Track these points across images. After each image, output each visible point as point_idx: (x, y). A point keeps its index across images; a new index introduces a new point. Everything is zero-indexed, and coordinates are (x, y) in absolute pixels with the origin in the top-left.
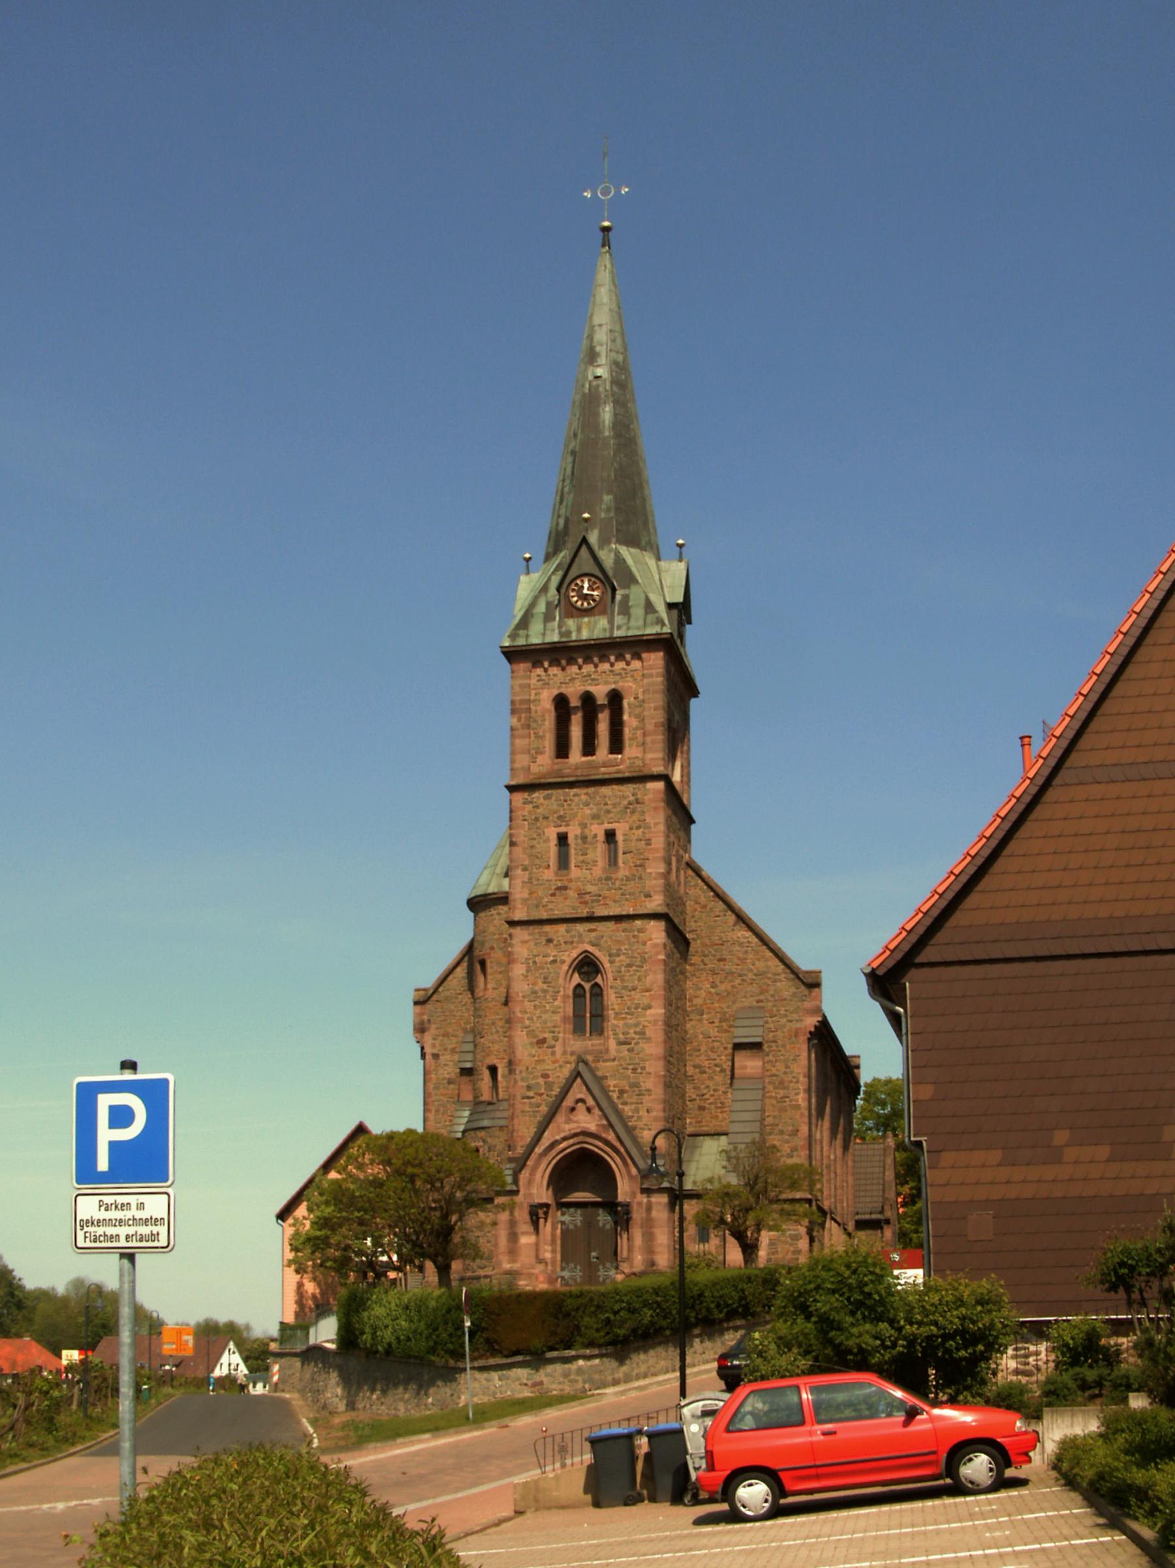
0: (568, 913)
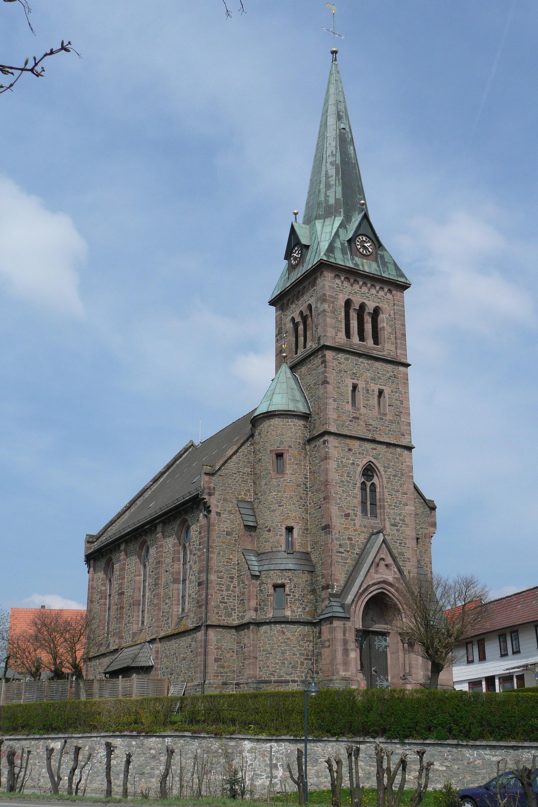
0: (360, 434)
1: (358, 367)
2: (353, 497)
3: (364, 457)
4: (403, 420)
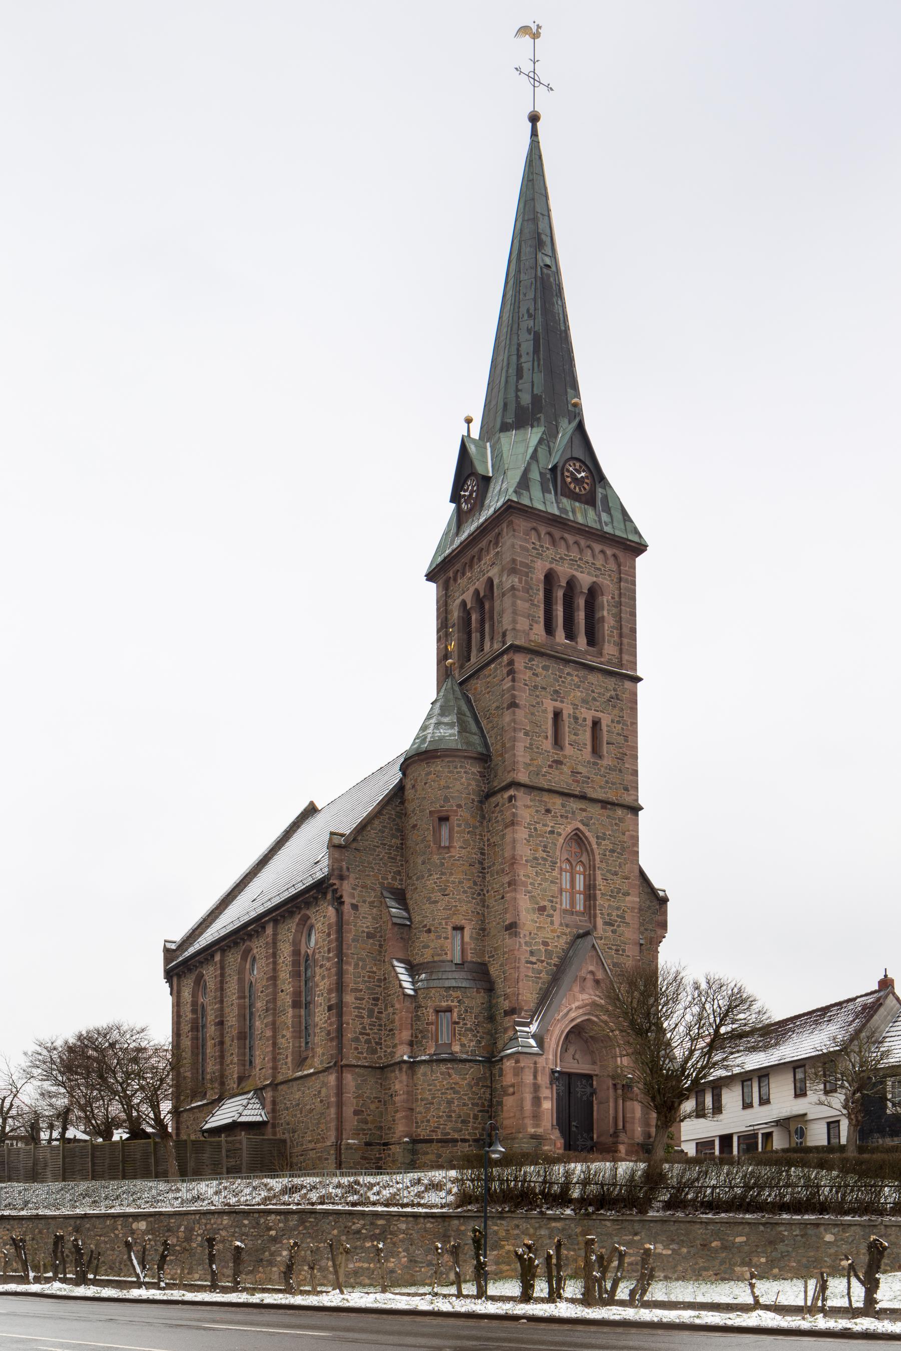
0: (563, 787)
1: (563, 682)
2: (552, 882)
3: (570, 823)
4: (627, 766)
